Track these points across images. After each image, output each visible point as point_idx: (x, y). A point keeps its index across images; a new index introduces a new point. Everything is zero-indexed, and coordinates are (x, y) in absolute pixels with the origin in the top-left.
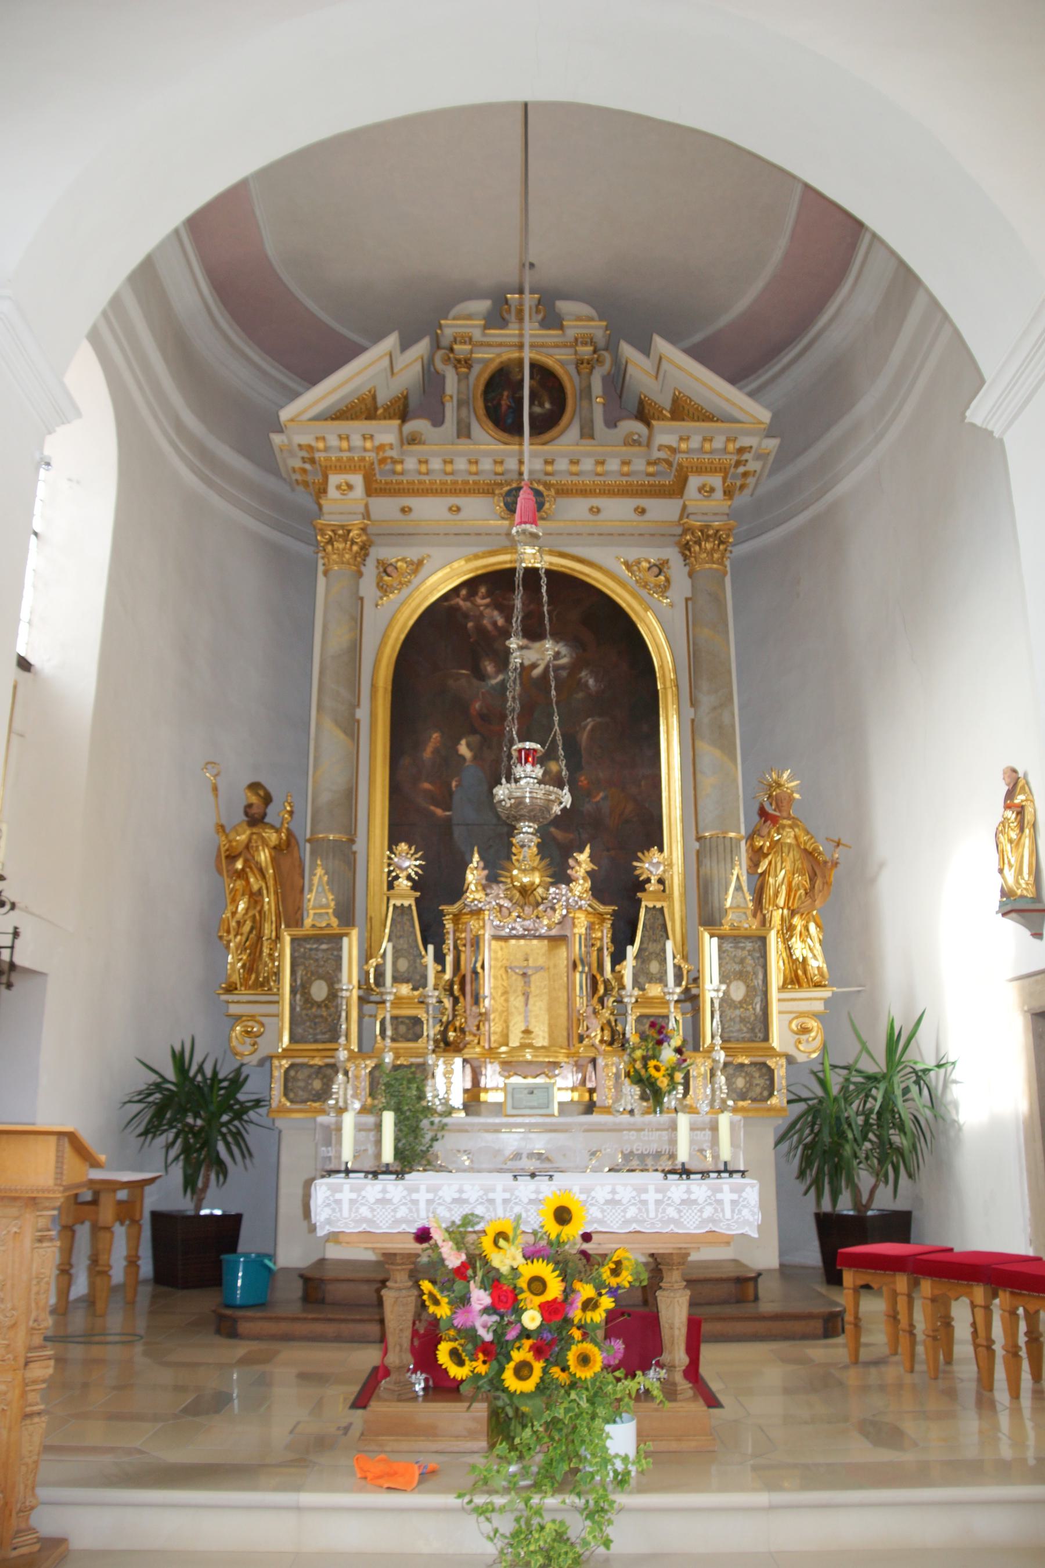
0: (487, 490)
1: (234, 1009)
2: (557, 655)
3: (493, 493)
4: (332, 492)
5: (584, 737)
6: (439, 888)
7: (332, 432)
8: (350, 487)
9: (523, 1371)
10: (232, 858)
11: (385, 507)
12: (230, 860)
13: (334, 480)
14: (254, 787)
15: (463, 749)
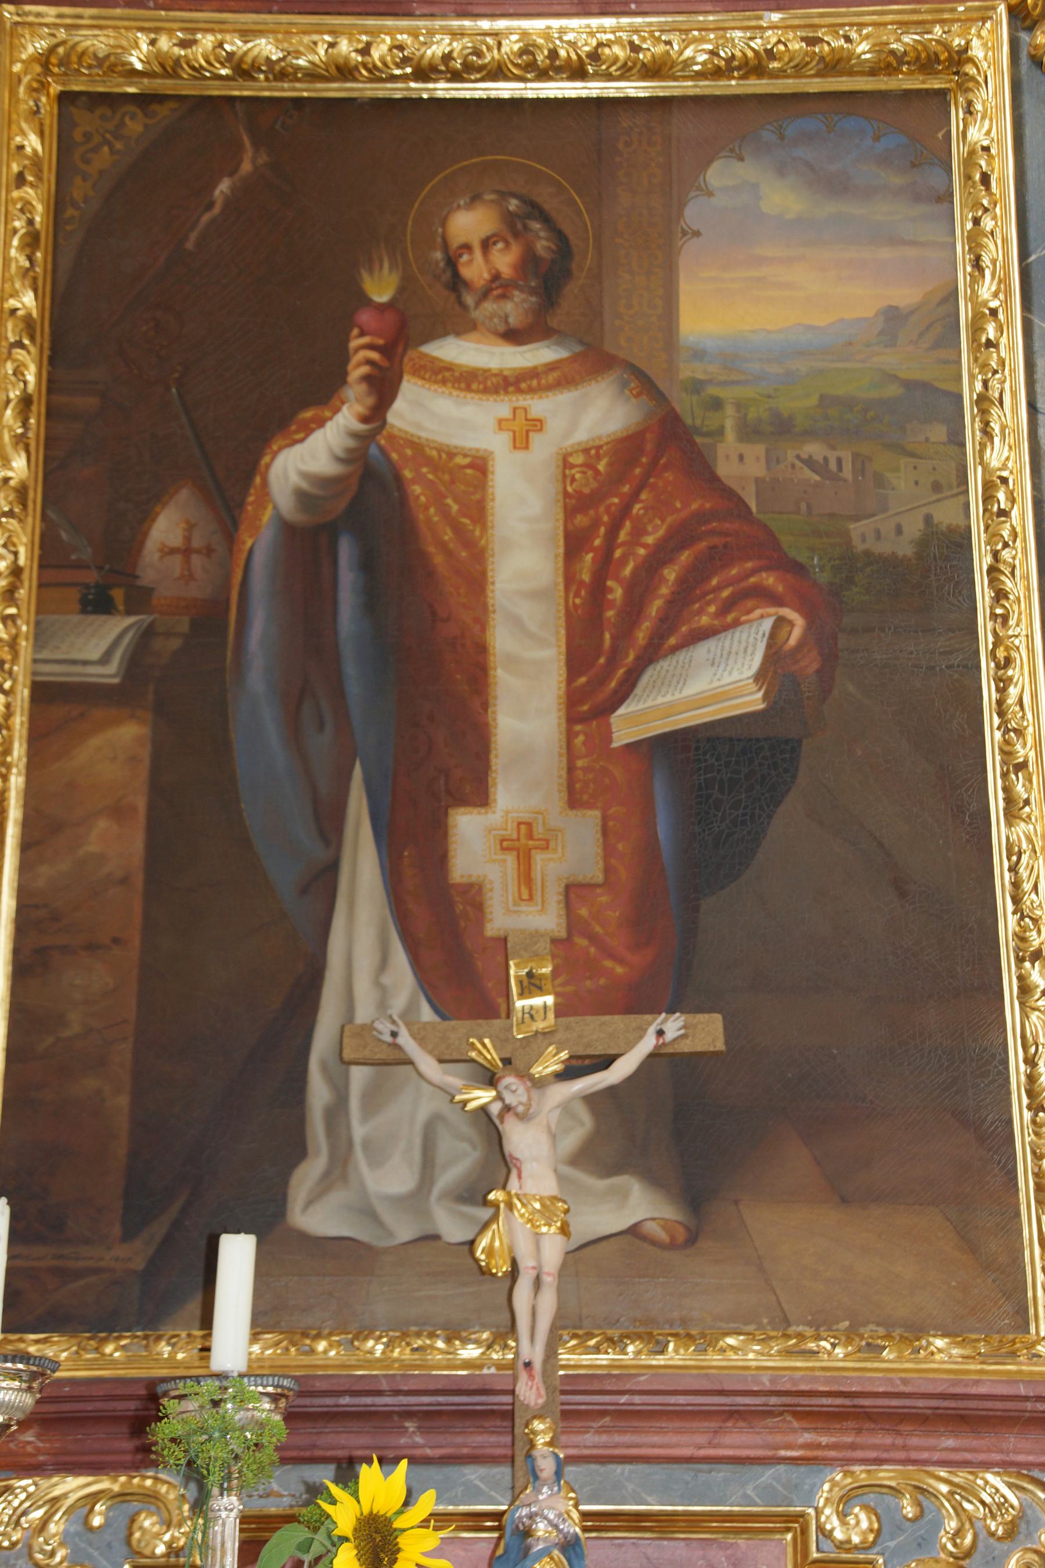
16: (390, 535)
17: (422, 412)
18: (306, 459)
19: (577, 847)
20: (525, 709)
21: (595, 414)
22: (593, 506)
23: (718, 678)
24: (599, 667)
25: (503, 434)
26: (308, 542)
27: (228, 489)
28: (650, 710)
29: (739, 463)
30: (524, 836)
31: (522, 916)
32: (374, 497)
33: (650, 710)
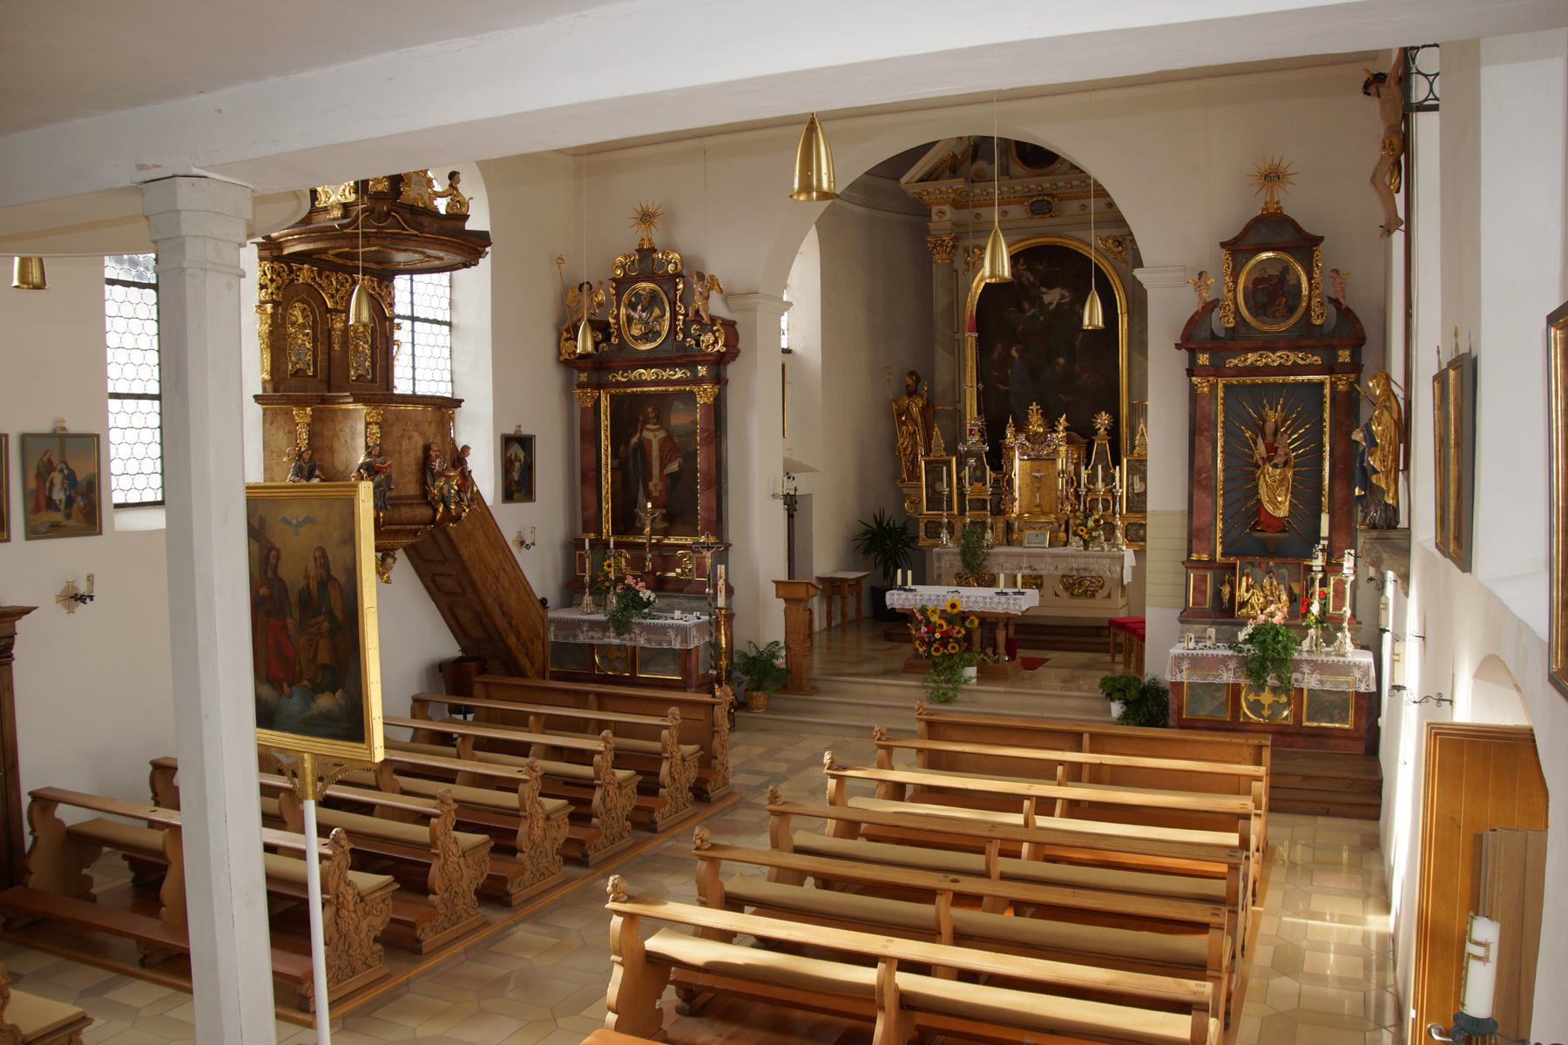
0: (1019, 201)
1: (905, 491)
2: (1063, 297)
3: (912, 393)
4: (935, 218)
5: (1078, 344)
6: (994, 434)
7: (930, 186)
8: (943, 213)
9: (937, 650)
10: (899, 415)
11: (966, 215)
12: (898, 415)
13: (935, 209)
14: (912, 374)
15: (1014, 353)
16: (643, 448)
17: (647, 434)
18: (634, 440)
19: (660, 487)
20: (656, 470)
21: (662, 434)
22: (663, 444)
23: (674, 467)
24: (663, 466)
25: (653, 436)
26: (635, 450)
27: (627, 444)
28: (666, 471)
29: (676, 440)
30: (656, 485)
31: (656, 494)
32: (641, 441)
33: (666, 471)
